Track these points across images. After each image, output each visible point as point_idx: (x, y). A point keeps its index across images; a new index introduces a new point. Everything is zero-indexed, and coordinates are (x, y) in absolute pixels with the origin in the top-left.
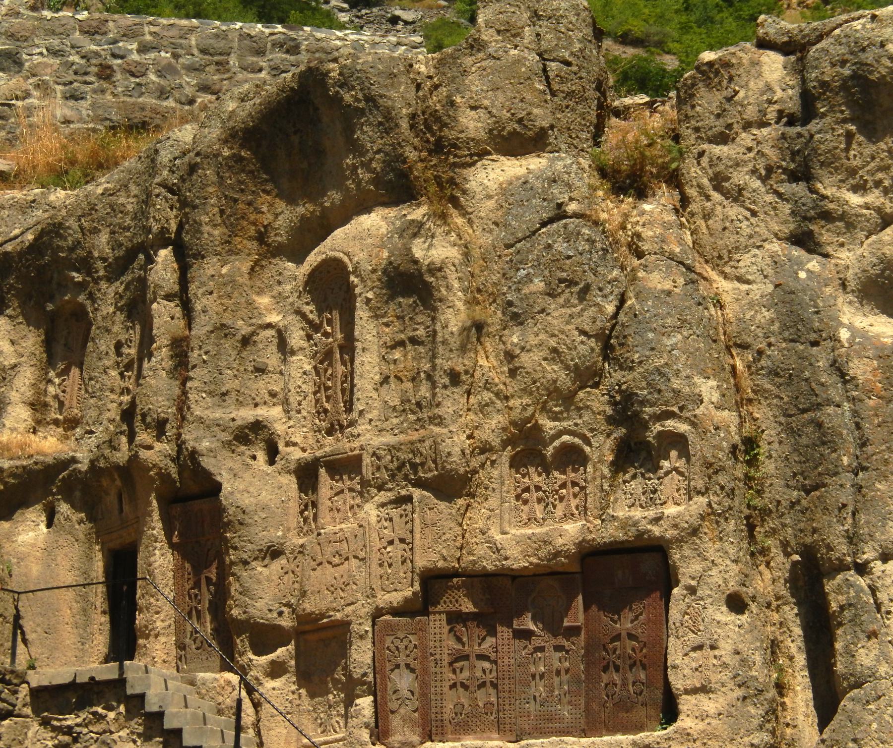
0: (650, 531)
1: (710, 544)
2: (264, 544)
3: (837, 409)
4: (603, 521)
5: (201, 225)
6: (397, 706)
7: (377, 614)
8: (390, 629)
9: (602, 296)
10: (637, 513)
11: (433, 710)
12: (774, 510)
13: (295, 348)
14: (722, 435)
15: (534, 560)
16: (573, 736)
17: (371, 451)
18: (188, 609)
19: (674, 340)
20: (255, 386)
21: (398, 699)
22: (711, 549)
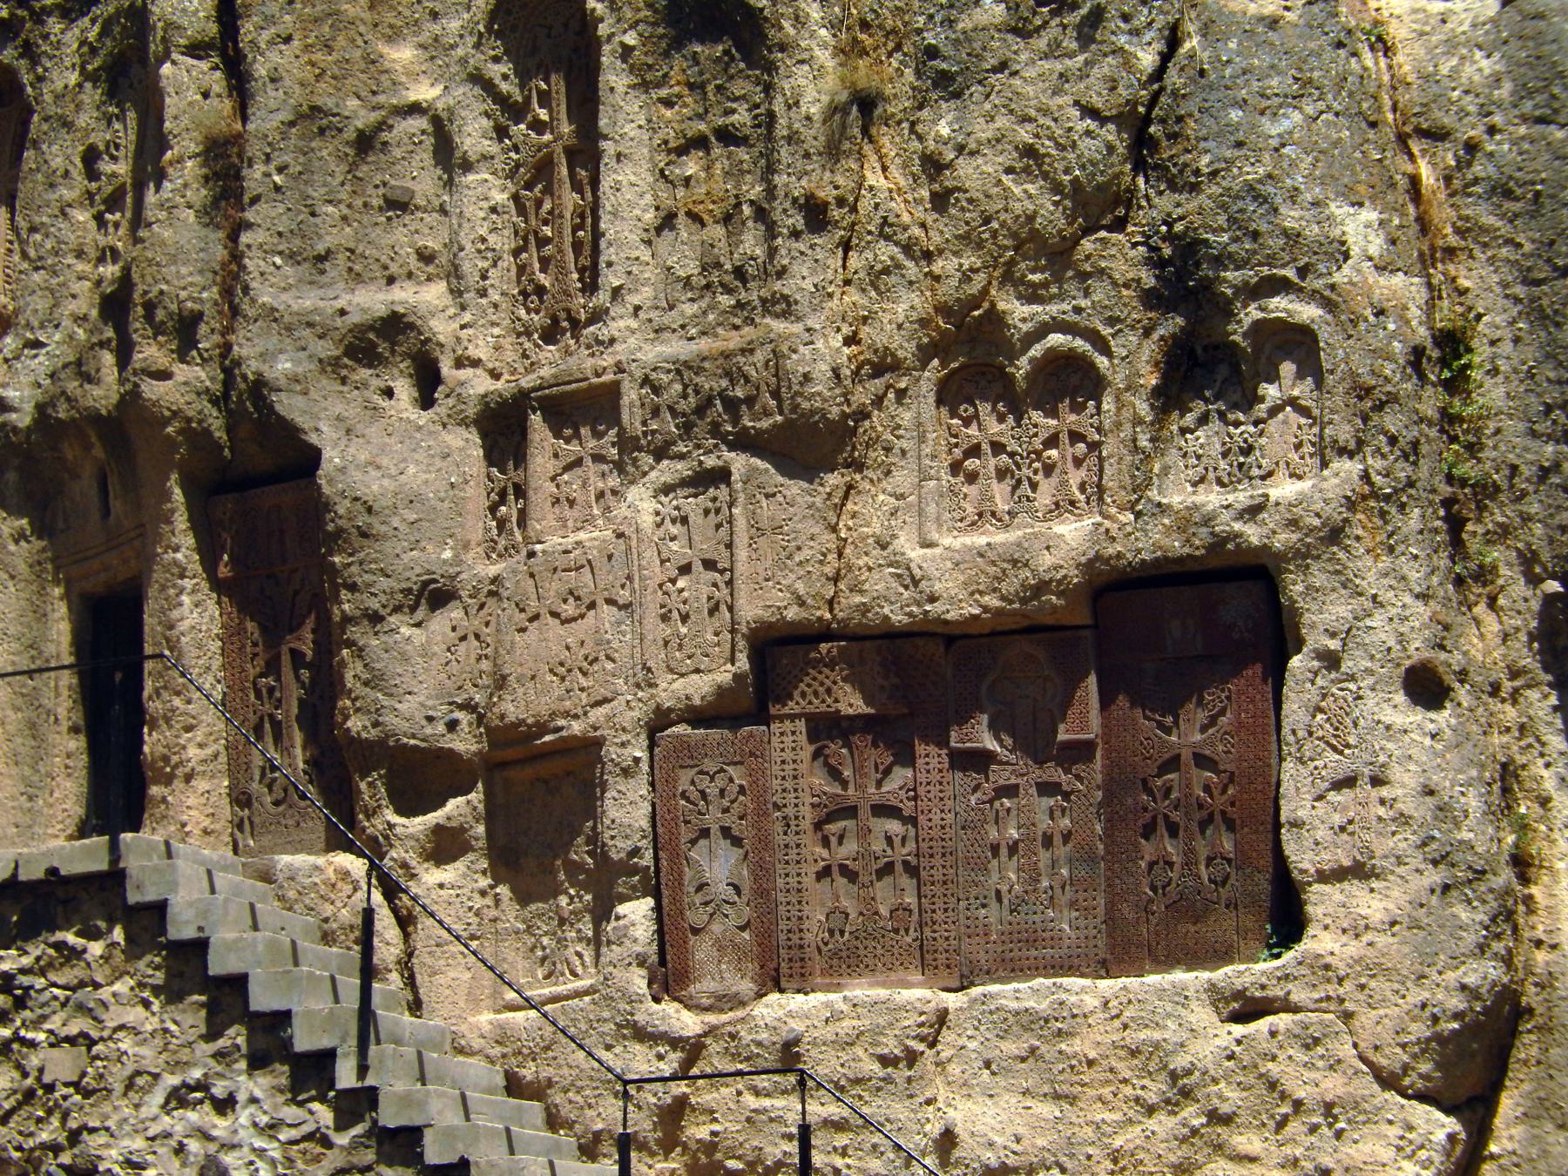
0: (1238, 535)
1: (1369, 561)
2: (413, 578)
4: (1138, 515)
6: (706, 918)
7: (658, 723)
8: (687, 754)
9: (1130, 33)
10: (1211, 498)
11: (783, 925)
12: (1504, 485)
13: (473, 157)
14: (1391, 327)
15: (993, 601)
16: (1082, 975)
17: (638, 374)
18: (253, 719)
19: (1286, 124)
20: (387, 240)
21: (706, 904)
22: (1370, 571)
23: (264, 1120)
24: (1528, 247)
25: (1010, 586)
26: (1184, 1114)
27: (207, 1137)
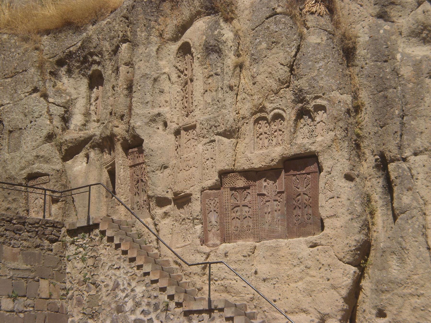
3: (394, 90)
4: (291, 145)
5: (137, 32)
7: (203, 190)
8: (208, 196)
9: (289, 48)
10: (306, 141)
11: (225, 230)
12: (368, 137)
13: (174, 82)
14: (342, 105)
15: (264, 164)
16: (283, 239)
17: (200, 122)
19: (321, 64)
20: (160, 99)
22: (337, 155)
23: (125, 271)
24: (373, 87)
25: (267, 160)
26: (301, 267)
27: (115, 275)
